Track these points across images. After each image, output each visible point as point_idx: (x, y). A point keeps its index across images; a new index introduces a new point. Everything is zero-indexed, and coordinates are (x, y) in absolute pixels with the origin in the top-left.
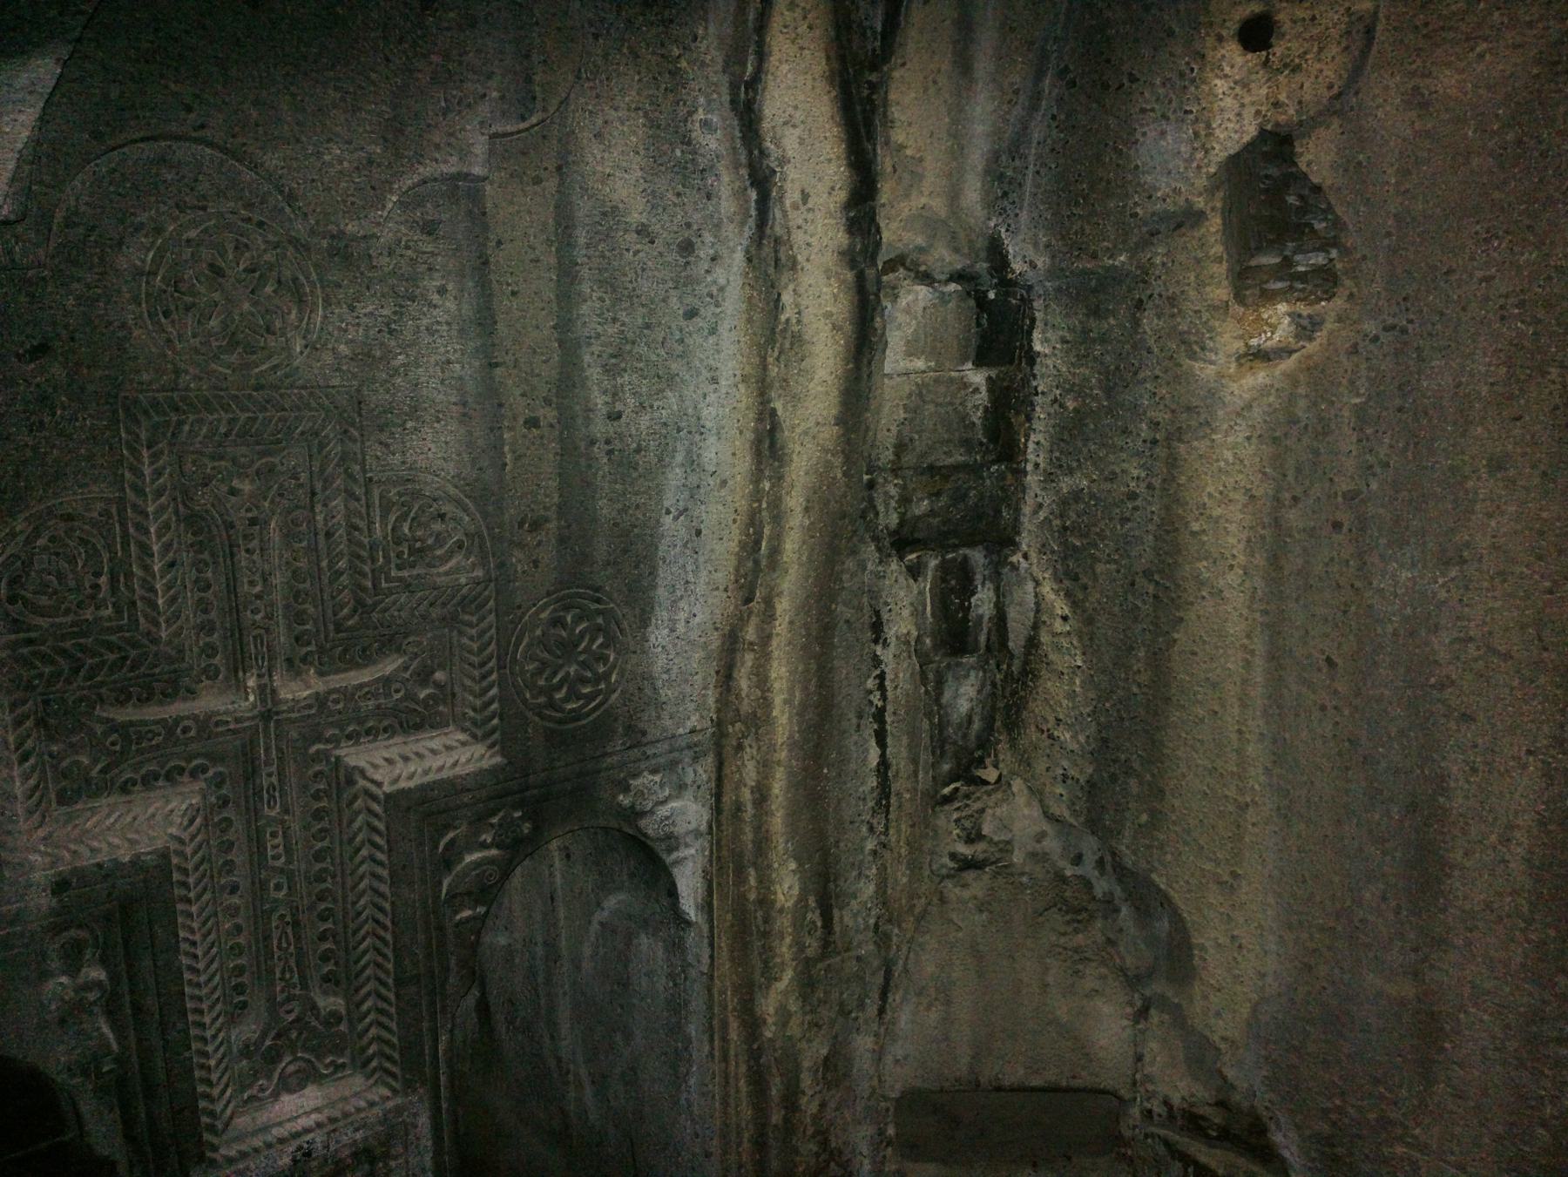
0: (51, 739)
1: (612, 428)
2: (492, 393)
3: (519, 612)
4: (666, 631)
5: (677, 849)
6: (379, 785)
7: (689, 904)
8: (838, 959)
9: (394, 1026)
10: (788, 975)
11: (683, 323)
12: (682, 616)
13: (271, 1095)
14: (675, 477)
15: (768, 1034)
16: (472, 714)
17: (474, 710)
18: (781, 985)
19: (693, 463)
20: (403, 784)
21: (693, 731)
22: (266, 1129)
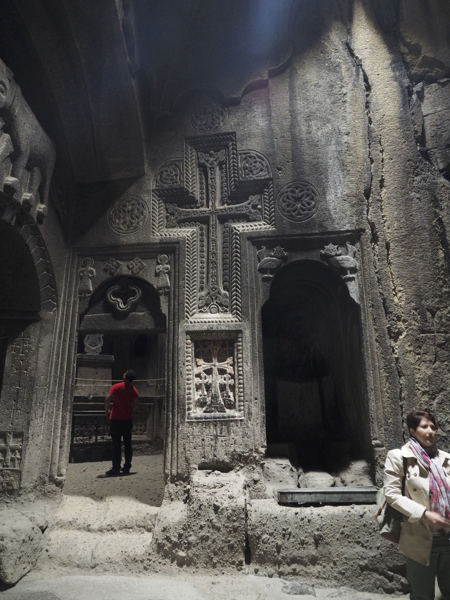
0: (168, 213)
1: (309, 135)
2: (271, 130)
3: (280, 187)
4: (333, 196)
5: (347, 274)
6: (239, 231)
7: (354, 295)
8: (433, 334)
9: (240, 300)
10: (405, 333)
11: (331, 106)
12: (339, 191)
13: (206, 312)
14: (333, 148)
15: (396, 356)
16: (267, 216)
17: (268, 215)
18: (401, 337)
19: (338, 143)
20: (245, 231)
21: (347, 231)
22: (203, 318)
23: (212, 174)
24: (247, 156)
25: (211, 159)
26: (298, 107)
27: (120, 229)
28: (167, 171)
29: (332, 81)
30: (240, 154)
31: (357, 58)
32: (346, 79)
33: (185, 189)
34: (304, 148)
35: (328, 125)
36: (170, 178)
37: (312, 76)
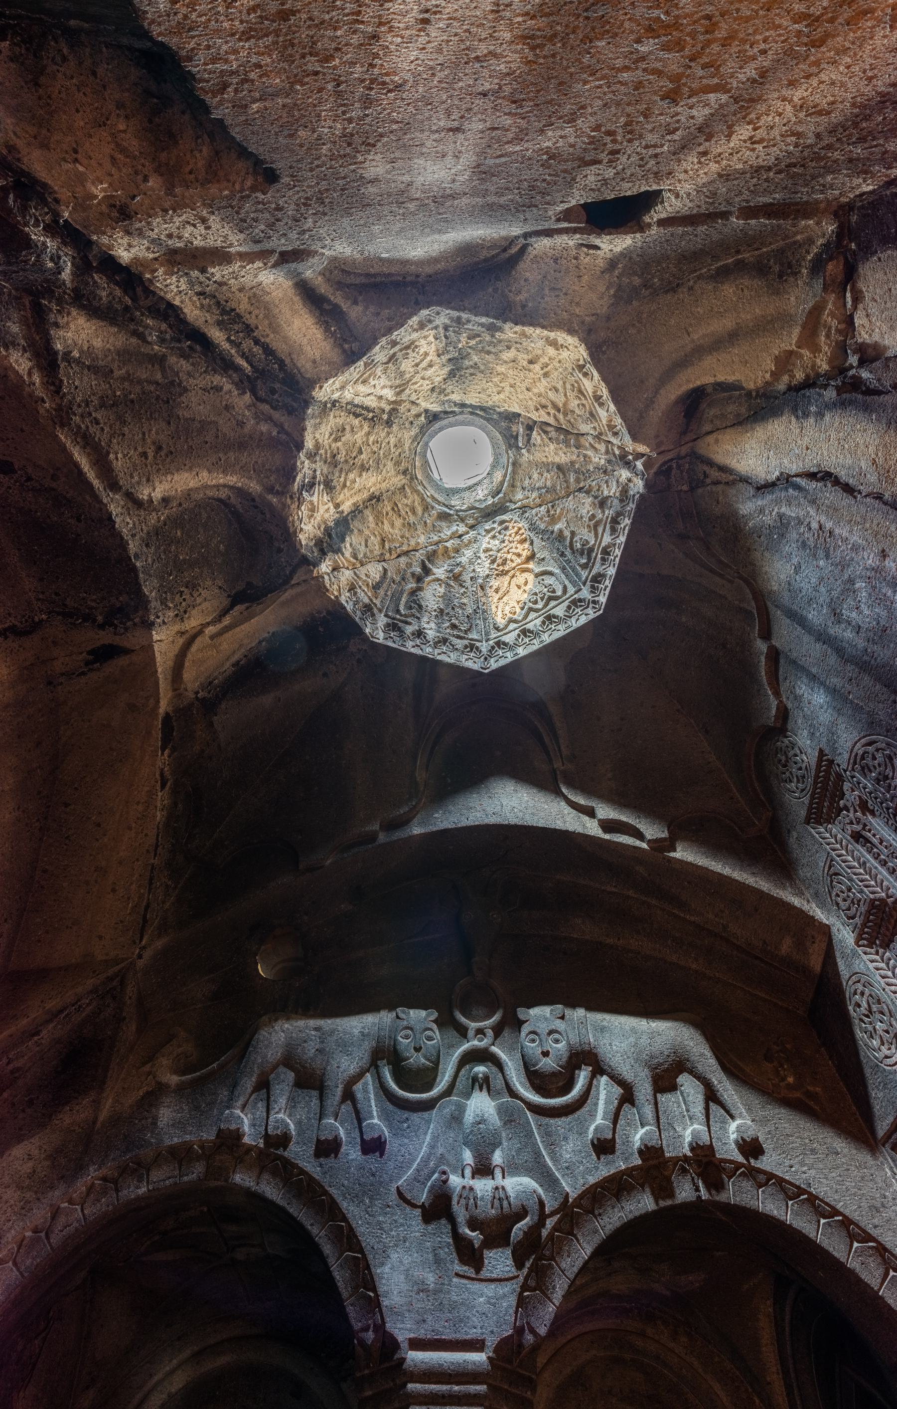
1: (862, 635)
11: (830, 561)
23: (874, 835)
24: (860, 762)
25: (851, 815)
26: (816, 621)
27: (887, 1057)
28: (838, 895)
29: (797, 541)
30: (853, 770)
31: (778, 479)
32: (801, 513)
33: (875, 900)
34: (879, 655)
35: (857, 586)
36: (849, 902)
37: (786, 570)
